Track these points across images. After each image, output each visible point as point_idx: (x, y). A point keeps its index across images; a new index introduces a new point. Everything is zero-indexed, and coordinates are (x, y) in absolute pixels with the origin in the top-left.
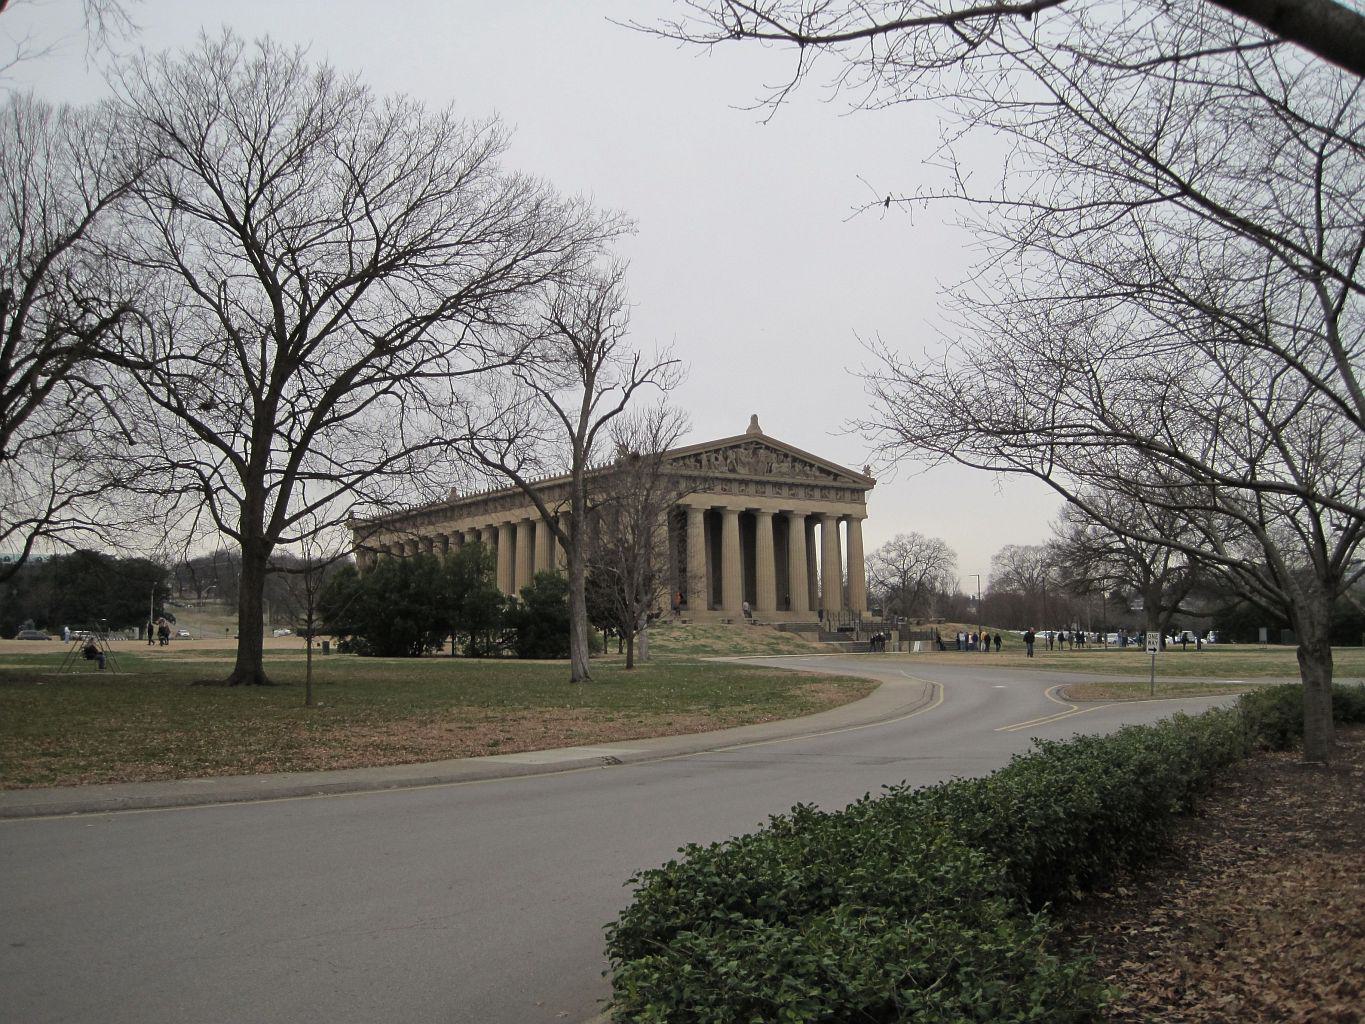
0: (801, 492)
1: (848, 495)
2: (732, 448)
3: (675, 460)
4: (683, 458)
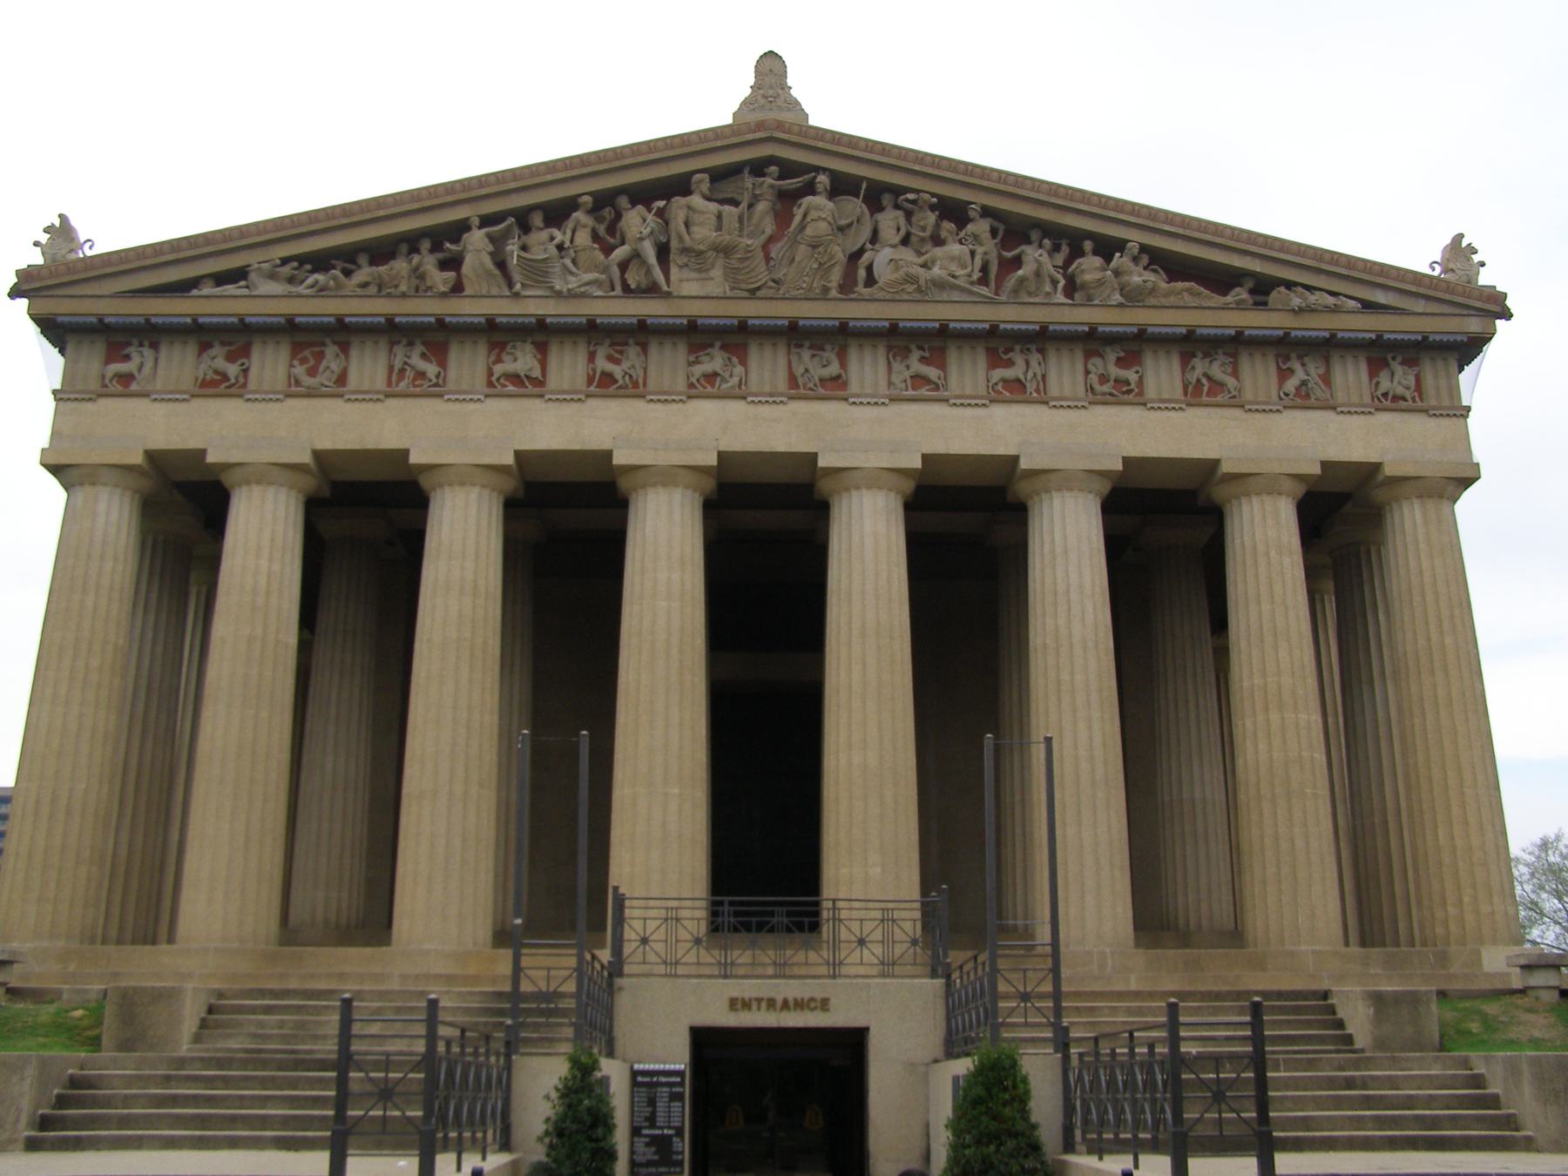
0: (1065, 372)
1: (1350, 376)
2: (642, 195)
3: (319, 262)
4: (381, 252)
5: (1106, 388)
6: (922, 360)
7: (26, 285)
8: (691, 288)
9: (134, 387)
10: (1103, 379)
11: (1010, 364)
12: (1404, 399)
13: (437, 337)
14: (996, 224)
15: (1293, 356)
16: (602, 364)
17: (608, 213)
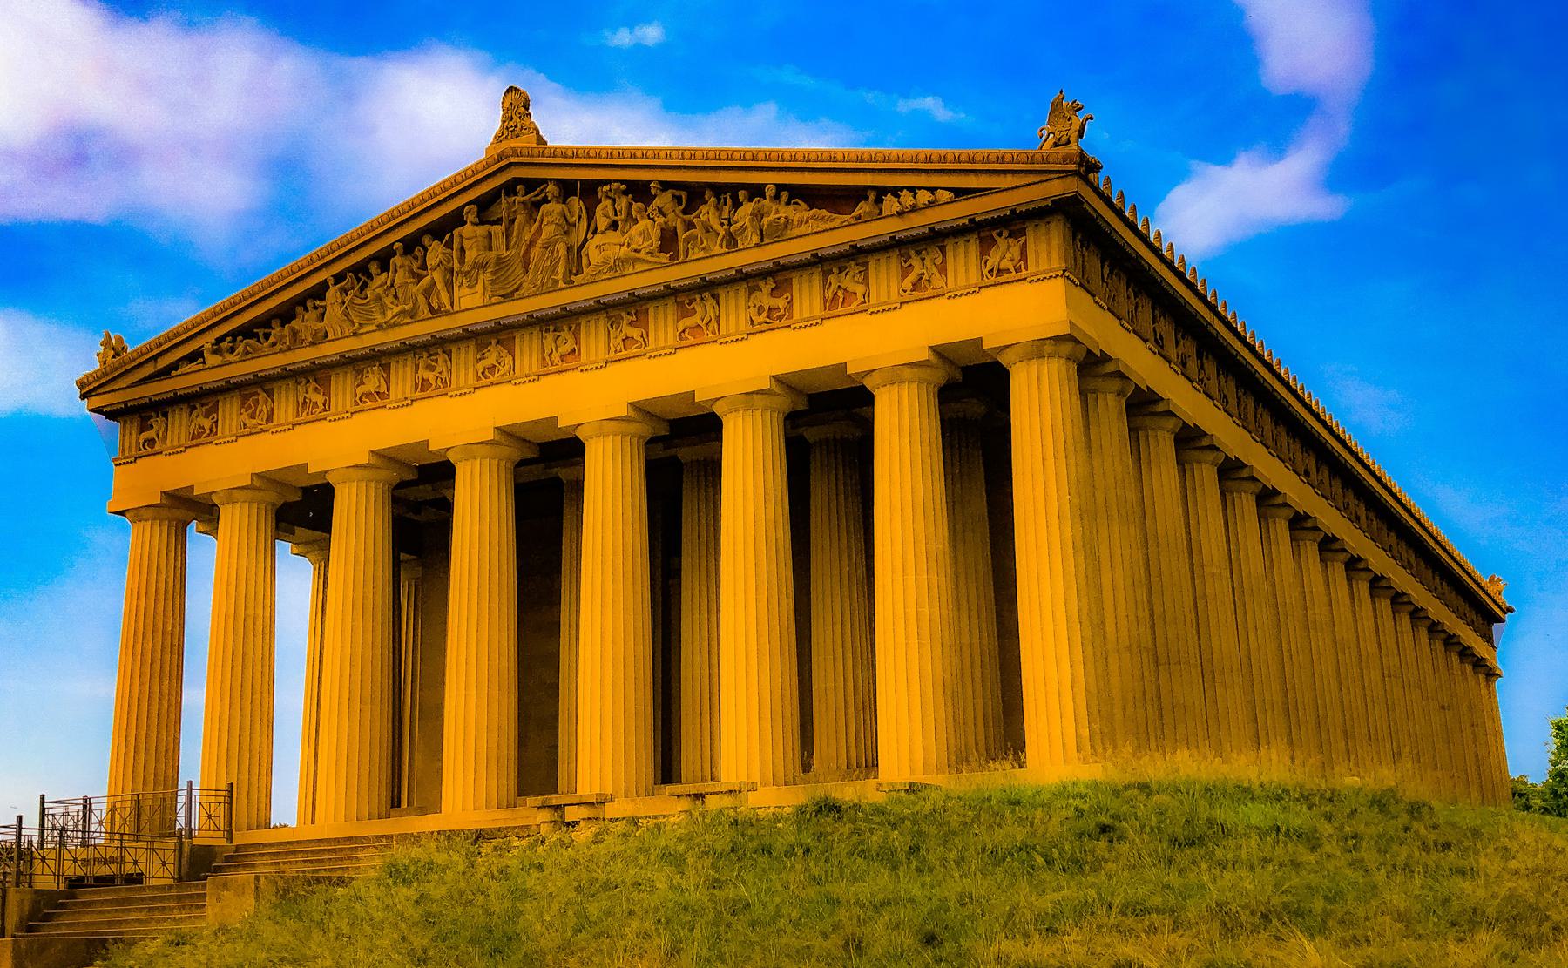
3: (247, 331)
4: (286, 314)
5: (763, 318)
6: (631, 324)
8: (466, 303)
9: (157, 447)
10: (760, 310)
11: (694, 312)
12: (1008, 271)
13: (317, 374)
14: (677, 193)
15: (912, 252)
16: (424, 373)
17: (418, 251)
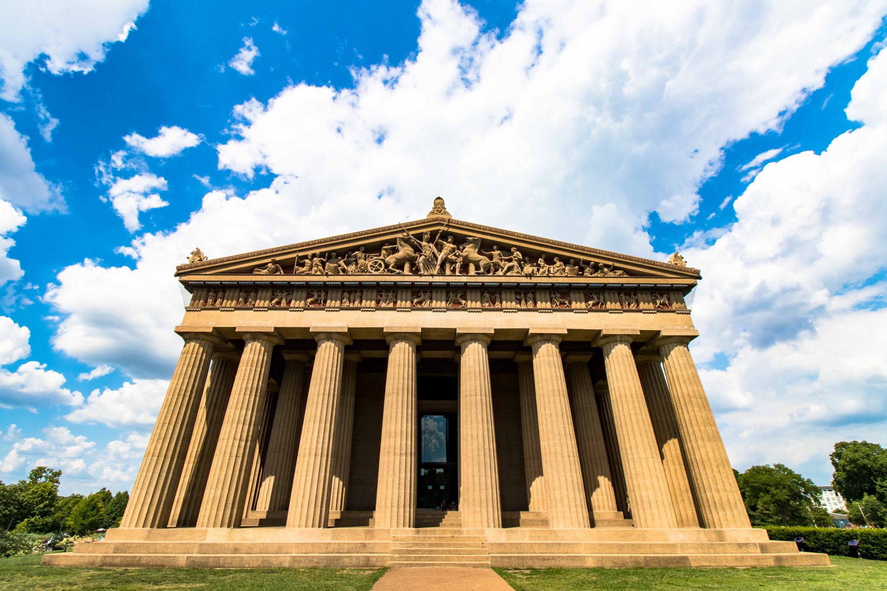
7: (181, 272)
